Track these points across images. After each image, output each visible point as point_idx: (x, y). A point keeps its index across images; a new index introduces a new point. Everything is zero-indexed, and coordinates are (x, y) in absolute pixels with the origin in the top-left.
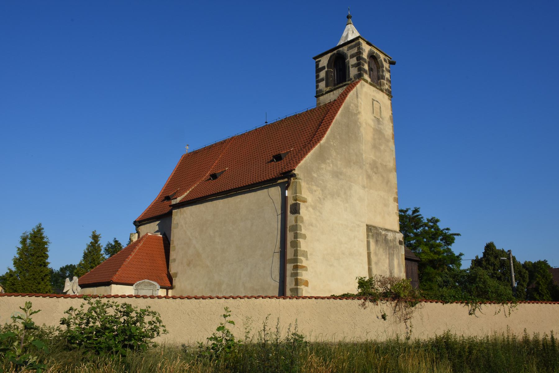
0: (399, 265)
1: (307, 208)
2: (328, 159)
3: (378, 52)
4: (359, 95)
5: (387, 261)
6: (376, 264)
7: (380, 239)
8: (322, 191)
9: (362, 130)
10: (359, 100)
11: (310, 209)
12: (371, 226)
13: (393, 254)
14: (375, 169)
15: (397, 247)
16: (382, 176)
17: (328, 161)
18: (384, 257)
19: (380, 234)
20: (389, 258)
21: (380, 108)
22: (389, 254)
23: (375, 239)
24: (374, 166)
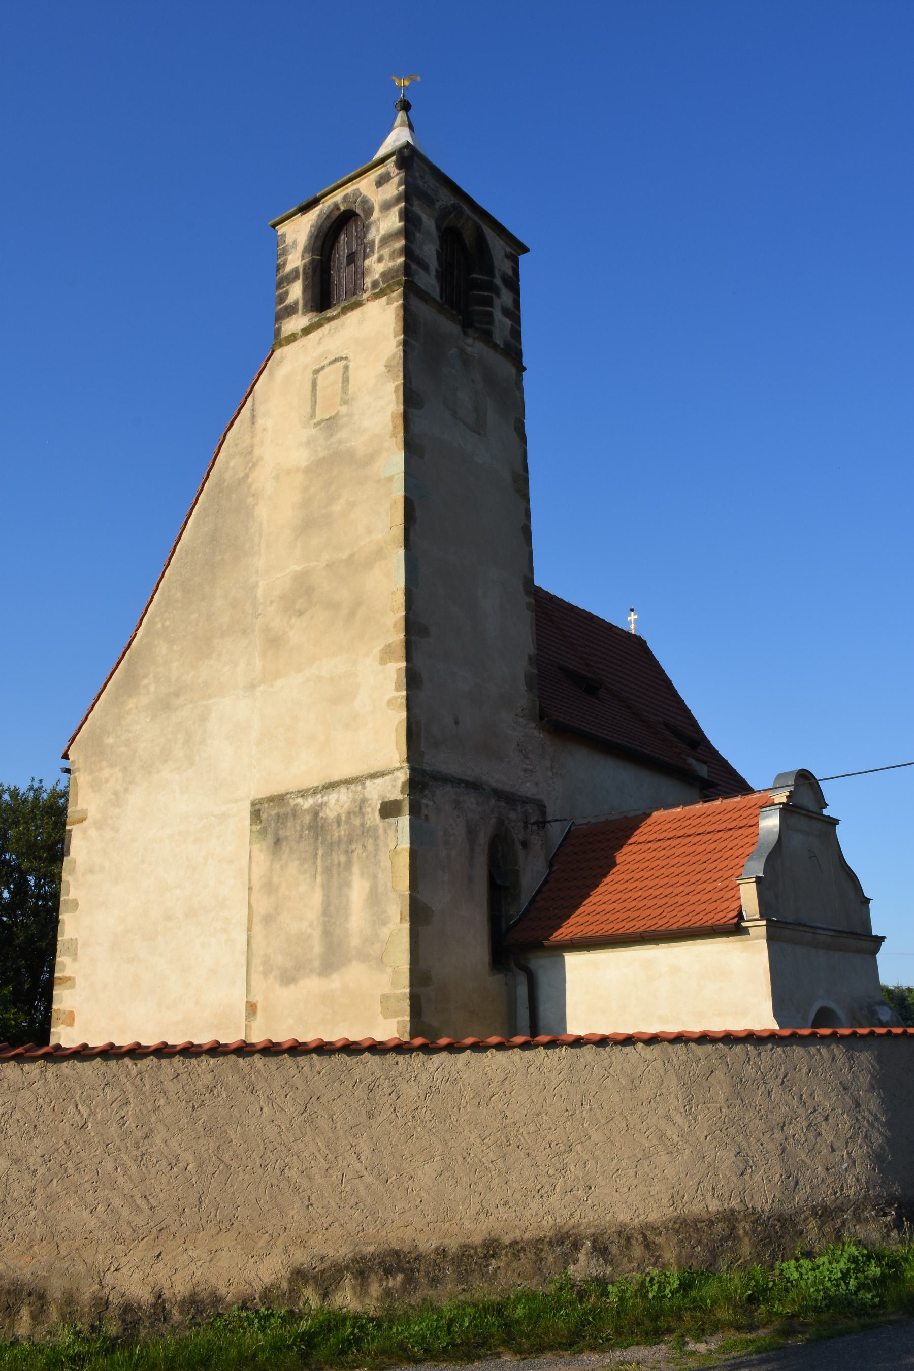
0: (374, 899)
1: (85, 832)
2: (145, 676)
3: (350, 189)
4: (260, 409)
5: (317, 898)
6: (268, 919)
7: (290, 830)
8: (125, 769)
9: (262, 511)
10: (260, 422)
11: (93, 832)
12: (261, 801)
13: (348, 865)
14: (300, 604)
15: (367, 832)
16: (333, 606)
17: (145, 682)
18: (303, 888)
19: (295, 813)
20: (326, 887)
21: (346, 368)
22: (327, 871)
23: (270, 839)
24: (301, 596)
